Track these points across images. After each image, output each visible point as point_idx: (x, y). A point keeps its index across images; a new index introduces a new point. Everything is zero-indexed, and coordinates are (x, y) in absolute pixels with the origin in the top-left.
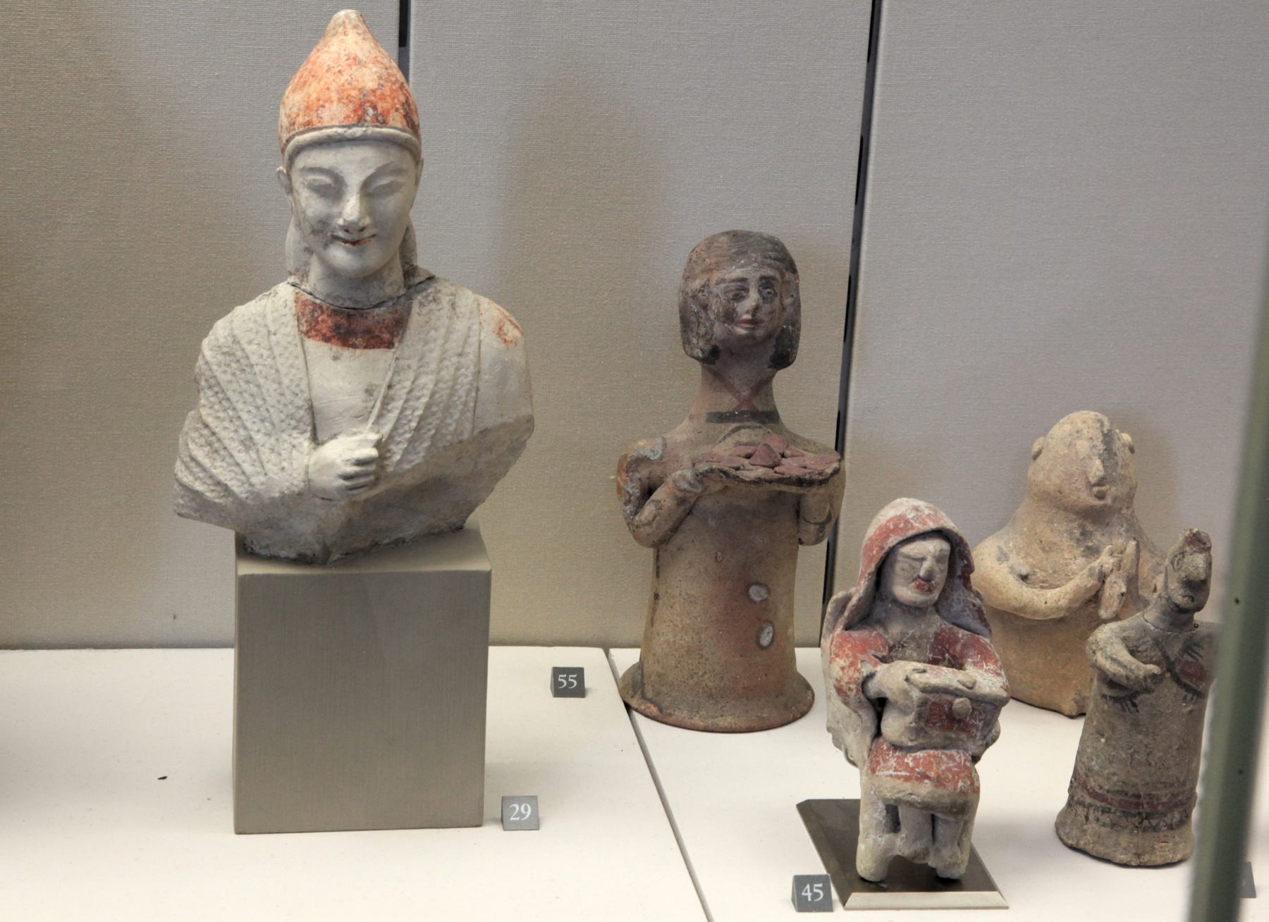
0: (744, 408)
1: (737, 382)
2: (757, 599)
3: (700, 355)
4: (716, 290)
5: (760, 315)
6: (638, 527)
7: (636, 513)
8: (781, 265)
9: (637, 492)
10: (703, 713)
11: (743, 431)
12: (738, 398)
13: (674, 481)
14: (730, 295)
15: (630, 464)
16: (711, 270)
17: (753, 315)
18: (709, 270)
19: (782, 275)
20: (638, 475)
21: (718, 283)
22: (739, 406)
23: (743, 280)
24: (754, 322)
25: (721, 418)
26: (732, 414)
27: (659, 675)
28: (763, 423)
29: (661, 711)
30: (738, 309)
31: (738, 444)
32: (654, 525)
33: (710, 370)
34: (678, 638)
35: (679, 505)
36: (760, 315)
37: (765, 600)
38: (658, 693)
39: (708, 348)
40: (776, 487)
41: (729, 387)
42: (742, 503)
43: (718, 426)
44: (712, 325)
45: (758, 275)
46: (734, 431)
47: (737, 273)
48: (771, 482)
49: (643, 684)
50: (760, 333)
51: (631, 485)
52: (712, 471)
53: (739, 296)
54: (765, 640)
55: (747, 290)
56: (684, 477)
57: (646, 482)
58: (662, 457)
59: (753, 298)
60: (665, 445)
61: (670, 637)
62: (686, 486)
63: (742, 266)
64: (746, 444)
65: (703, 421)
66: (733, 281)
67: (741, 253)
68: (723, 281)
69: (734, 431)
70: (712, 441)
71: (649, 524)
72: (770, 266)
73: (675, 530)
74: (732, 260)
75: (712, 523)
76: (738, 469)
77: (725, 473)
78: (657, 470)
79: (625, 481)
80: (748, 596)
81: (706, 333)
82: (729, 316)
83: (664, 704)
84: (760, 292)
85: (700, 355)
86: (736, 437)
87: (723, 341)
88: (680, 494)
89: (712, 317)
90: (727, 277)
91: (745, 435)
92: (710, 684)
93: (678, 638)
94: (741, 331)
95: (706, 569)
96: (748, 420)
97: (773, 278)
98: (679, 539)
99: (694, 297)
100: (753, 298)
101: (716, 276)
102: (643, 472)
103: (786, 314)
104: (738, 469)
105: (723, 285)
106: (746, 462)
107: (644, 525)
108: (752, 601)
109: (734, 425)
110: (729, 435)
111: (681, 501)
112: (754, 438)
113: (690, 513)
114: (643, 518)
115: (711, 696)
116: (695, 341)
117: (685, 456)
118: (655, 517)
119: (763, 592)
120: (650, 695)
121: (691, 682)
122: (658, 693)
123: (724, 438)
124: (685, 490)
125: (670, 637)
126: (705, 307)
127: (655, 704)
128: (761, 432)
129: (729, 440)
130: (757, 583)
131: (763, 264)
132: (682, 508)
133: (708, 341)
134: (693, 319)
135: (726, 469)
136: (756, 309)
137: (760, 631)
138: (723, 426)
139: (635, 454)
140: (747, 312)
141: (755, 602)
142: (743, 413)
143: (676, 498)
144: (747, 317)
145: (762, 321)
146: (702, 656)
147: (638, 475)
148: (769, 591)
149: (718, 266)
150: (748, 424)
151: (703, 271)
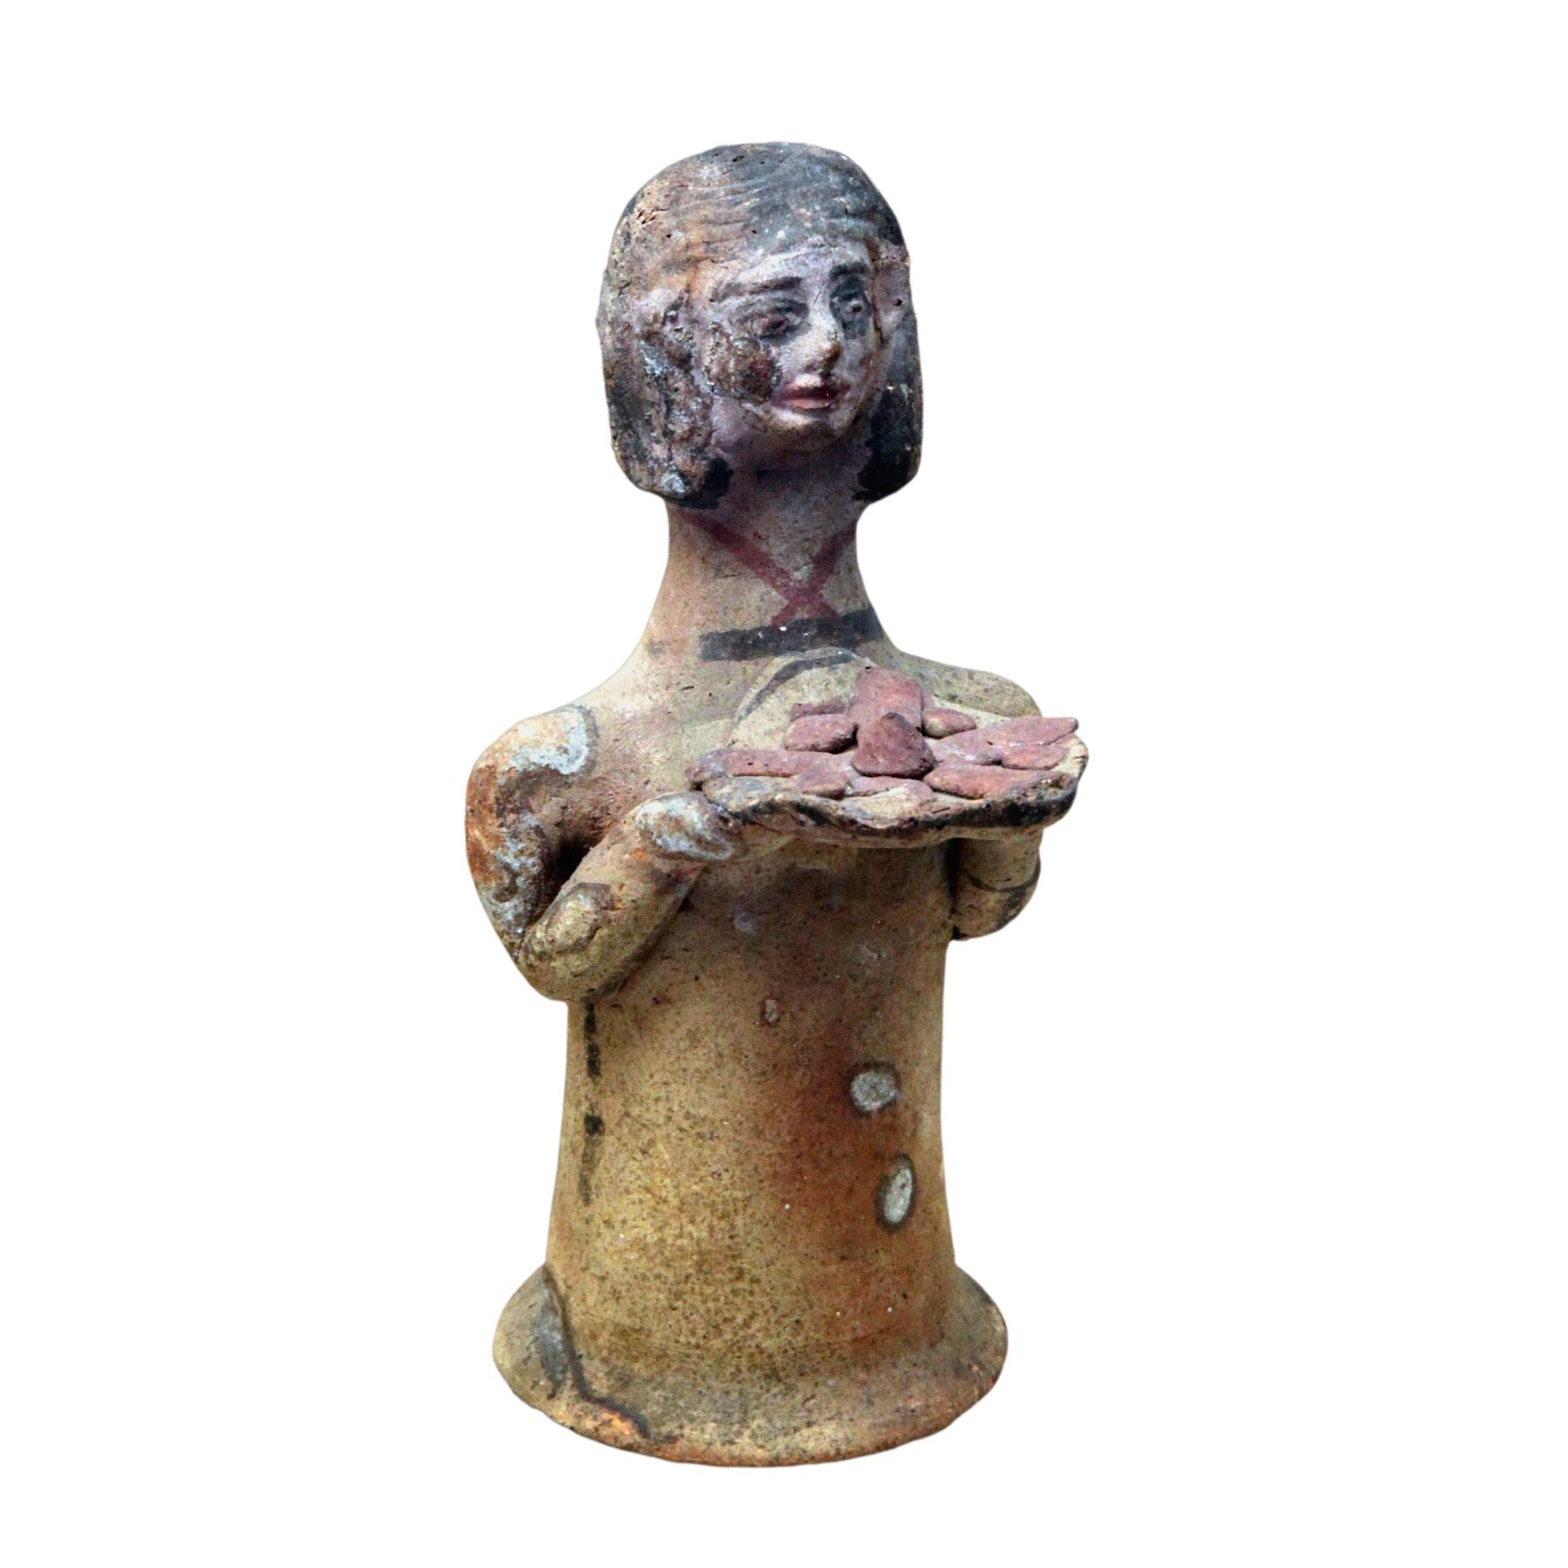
0: (802, 614)
1: (776, 548)
2: (873, 1105)
3: (679, 487)
4: (711, 315)
5: (842, 373)
6: (541, 956)
7: (532, 918)
8: (862, 225)
9: (533, 865)
10: (758, 1422)
11: (805, 675)
12: (784, 589)
13: (646, 833)
14: (757, 327)
15: (507, 793)
16: (693, 263)
17: (826, 376)
18: (689, 263)
19: (873, 251)
20: (530, 820)
21: (717, 297)
22: (789, 610)
23: (790, 284)
24: (827, 392)
25: (743, 645)
26: (772, 631)
27: (623, 1333)
28: (851, 644)
29: (643, 1430)
30: (784, 363)
31: (800, 712)
32: (594, 950)
33: (701, 523)
34: (670, 1233)
35: (661, 893)
36: (842, 373)
37: (892, 1103)
38: (625, 1381)
39: (701, 467)
40: (952, 833)
41: (759, 564)
42: (821, 865)
43: (736, 666)
44: (707, 407)
45: (826, 265)
46: (782, 678)
47: (768, 266)
48: (940, 824)
49: (574, 1358)
50: (841, 417)
51: (513, 847)
52: (772, 807)
53: (781, 328)
54: (896, 1208)
55: (801, 309)
56: (677, 824)
57: (554, 834)
58: (591, 764)
59: (820, 330)
60: (593, 731)
61: (647, 1231)
62: (684, 845)
63: (784, 247)
64: (821, 710)
65: (691, 659)
66: (764, 288)
67: (771, 210)
68: (734, 289)
69: (782, 678)
70: (719, 707)
71: (579, 947)
72: (850, 236)
73: (647, 955)
74: (752, 231)
75: (745, 927)
76: (839, 795)
77: (813, 813)
78: (583, 802)
79: (498, 841)
80: (851, 1101)
81: (692, 431)
82: (759, 382)
83: (650, 1411)
84: (835, 311)
85: (679, 487)
86: (790, 695)
87: (739, 445)
88: (665, 867)
89: (705, 385)
90: (745, 278)
91: (813, 686)
92: (768, 1344)
93: (670, 1233)
94: (792, 418)
95: (737, 1050)
96: (813, 643)
97: (860, 268)
98: (658, 976)
99: (649, 336)
100: (820, 330)
101: (711, 277)
102: (546, 811)
103: (889, 355)
104: (839, 795)
105: (733, 302)
106: (843, 764)
107: (562, 952)
108: (861, 1113)
109: (780, 662)
110: (770, 689)
111: (667, 883)
112: (838, 691)
113: (686, 906)
114: (558, 932)
115: (773, 1375)
116: (659, 451)
117: (653, 753)
118: (594, 929)
119: (886, 1086)
120: (601, 1387)
121: (716, 1344)
122: (625, 1381)
123: (759, 699)
124: (680, 855)
125: (647, 1231)
126: (684, 361)
127: (626, 1413)
128: (848, 672)
129: (771, 703)
130: (867, 1067)
131: (834, 234)
132: (670, 899)
133: (700, 450)
134: (651, 394)
135: (813, 800)
136: (834, 357)
137: (884, 1183)
138: (749, 666)
139: (518, 765)
140: (809, 369)
141: (868, 1114)
142: (804, 624)
143: (655, 875)
144: (811, 380)
145: (846, 387)
146: (740, 1275)
147: (530, 820)
148: (898, 1084)
149: (712, 251)
150: (817, 653)
151: (671, 266)
